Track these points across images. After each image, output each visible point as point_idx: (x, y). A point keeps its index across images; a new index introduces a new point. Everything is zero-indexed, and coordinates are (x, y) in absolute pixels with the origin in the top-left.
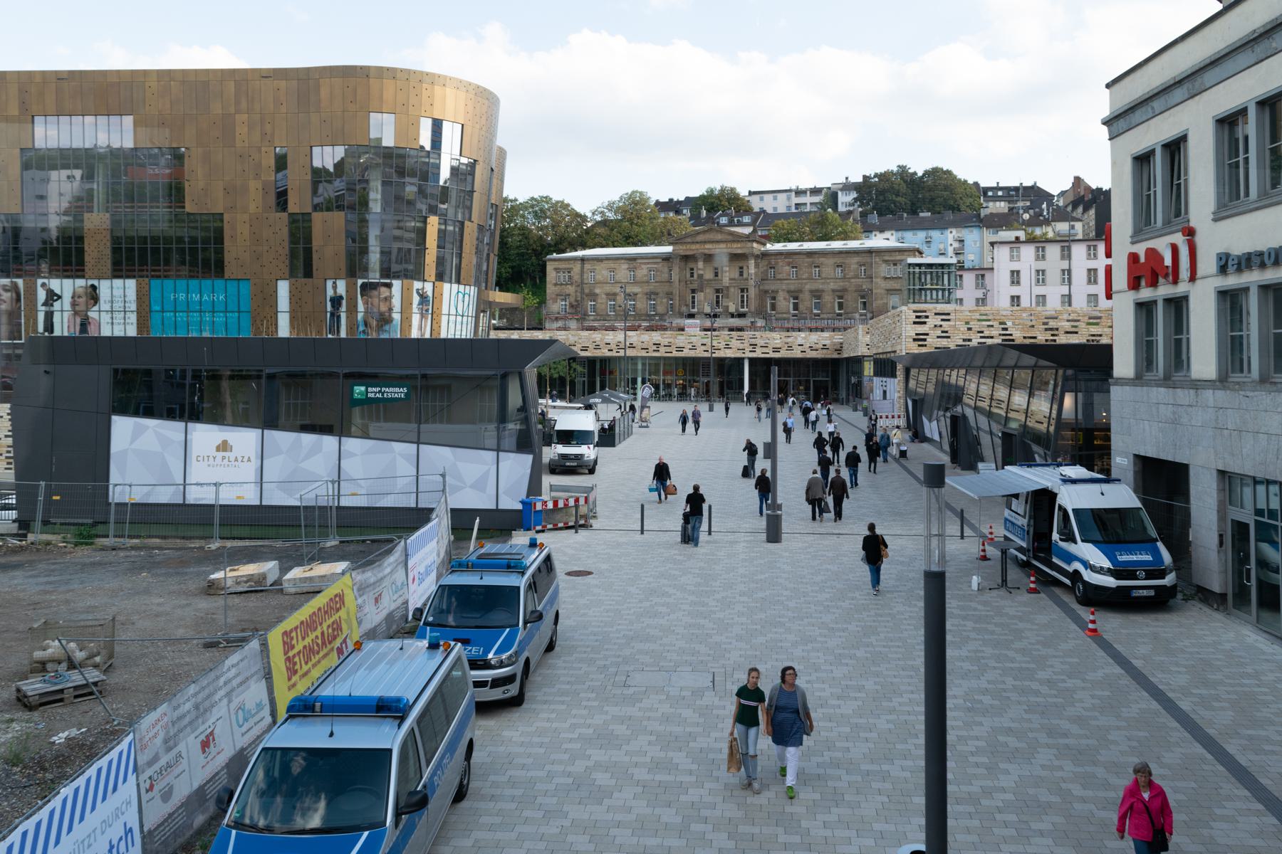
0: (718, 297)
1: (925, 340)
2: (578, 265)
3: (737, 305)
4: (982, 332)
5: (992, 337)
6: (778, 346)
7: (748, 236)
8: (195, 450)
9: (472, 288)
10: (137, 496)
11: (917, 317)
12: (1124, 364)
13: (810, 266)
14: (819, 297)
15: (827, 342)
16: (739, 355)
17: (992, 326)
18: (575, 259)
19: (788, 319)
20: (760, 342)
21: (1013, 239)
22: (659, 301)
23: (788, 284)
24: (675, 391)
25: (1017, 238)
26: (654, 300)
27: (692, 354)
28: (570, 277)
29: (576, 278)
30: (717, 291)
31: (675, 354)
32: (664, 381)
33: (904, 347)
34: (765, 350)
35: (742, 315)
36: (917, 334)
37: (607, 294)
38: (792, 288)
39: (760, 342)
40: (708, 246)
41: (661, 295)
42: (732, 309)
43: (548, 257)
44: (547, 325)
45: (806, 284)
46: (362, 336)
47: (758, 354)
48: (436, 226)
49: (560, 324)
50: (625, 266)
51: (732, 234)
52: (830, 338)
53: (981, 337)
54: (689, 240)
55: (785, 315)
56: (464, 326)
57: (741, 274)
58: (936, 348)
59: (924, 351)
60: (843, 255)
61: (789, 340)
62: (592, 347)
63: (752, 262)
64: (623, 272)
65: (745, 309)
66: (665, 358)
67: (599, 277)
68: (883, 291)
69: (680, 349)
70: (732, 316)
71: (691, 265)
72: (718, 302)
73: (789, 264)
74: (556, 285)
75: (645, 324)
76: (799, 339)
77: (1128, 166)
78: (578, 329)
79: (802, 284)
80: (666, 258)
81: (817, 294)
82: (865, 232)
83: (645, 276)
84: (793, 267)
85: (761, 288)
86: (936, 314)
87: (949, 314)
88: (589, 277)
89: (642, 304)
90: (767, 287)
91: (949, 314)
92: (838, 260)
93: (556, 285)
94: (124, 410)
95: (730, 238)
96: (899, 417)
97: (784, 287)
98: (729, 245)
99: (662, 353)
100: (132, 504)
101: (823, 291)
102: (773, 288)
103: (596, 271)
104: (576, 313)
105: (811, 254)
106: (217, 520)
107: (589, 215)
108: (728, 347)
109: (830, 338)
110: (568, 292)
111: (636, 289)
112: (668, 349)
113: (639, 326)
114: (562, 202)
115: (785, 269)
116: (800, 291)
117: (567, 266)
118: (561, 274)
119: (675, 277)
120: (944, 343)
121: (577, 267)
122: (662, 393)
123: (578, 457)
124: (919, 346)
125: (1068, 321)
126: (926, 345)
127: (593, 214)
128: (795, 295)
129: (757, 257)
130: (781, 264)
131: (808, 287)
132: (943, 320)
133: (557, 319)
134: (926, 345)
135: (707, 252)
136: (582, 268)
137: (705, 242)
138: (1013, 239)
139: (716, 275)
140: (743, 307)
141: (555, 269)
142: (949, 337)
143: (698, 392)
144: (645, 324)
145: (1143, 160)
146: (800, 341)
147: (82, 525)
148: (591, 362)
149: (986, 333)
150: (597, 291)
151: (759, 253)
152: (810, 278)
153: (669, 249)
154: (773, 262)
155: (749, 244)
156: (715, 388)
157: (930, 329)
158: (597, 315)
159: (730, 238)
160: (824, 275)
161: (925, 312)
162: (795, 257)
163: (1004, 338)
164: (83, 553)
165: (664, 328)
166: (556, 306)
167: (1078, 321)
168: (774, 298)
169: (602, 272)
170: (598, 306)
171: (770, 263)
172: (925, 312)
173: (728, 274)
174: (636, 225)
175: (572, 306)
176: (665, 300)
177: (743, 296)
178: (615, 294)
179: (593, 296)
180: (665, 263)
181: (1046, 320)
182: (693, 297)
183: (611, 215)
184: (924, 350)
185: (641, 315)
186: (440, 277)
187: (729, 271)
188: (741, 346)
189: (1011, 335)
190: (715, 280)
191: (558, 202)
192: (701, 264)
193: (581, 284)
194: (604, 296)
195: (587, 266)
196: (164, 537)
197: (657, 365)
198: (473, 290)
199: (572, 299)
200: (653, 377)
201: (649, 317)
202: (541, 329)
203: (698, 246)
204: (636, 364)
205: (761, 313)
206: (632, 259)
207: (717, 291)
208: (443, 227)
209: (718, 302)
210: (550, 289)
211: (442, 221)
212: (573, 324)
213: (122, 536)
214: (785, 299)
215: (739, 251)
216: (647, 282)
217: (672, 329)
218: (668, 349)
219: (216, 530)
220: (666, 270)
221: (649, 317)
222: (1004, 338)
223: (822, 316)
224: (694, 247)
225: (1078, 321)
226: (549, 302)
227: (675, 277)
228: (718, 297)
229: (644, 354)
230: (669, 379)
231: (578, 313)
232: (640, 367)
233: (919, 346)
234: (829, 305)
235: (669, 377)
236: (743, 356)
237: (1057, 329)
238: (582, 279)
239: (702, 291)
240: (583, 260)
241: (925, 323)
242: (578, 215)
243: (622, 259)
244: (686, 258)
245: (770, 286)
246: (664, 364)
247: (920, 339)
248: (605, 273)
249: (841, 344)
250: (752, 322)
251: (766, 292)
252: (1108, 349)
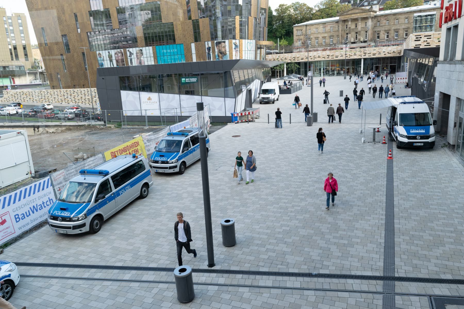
0: (356, 35)
2: (305, 28)
3: (364, 38)
6: (375, 53)
7: (369, 10)
8: (142, 100)
9: (253, 40)
10: (129, 114)
11: (417, 38)
13: (394, 19)
14: (397, 32)
15: (395, 50)
16: (359, 57)
18: (303, 25)
19: (384, 42)
20: (368, 52)
22: (334, 38)
23: (385, 28)
24: (336, 72)
26: (332, 38)
27: (341, 58)
28: (302, 33)
29: (304, 32)
30: (357, 33)
31: (335, 59)
32: (331, 69)
34: (370, 55)
35: (365, 42)
37: (315, 38)
38: (386, 29)
39: (368, 52)
40: (353, 15)
41: (335, 36)
42: (362, 40)
43: (294, 26)
44: (294, 51)
45: (392, 27)
46: (218, 60)
47: (367, 57)
48: (239, 20)
49: (298, 50)
50: (322, 26)
51: (362, 9)
52: (397, 48)
54: (345, 14)
55: (383, 40)
56: (251, 54)
57: (366, 25)
60: (409, 14)
61: (380, 50)
62: (305, 58)
63: (370, 20)
64: (321, 29)
66: (332, 60)
67: (312, 32)
69: (337, 57)
70: (362, 42)
71: (346, 24)
72: (356, 37)
73: (385, 19)
74: (297, 36)
75: (329, 48)
76: (384, 49)
78: (305, 52)
79: (390, 27)
80: (337, 22)
81: (397, 31)
82: (425, 2)
83: (329, 29)
84: (387, 21)
85: (374, 30)
86: (425, 36)
87: (430, 36)
88: (309, 32)
89: (328, 41)
90: (376, 30)
91: (430, 36)
92: (406, 16)
93: (297, 36)
94: (125, 89)
95: (361, 11)
96: (406, 78)
97: (383, 29)
98: (361, 14)
99: (330, 58)
100: (127, 116)
101: (399, 29)
102: (378, 30)
103: (311, 29)
104: (304, 46)
105: (395, 14)
106: (147, 120)
107: (313, 7)
108: (355, 55)
109: (397, 48)
110: (301, 38)
111: (326, 35)
112: (332, 57)
113: (327, 49)
114: (304, 3)
115: (384, 22)
116: (390, 30)
117: (301, 28)
118: (299, 32)
119: (340, 29)
121: (304, 28)
122: (331, 73)
123: (268, 98)
127: (315, 7)
128: (388, 32)
129: (372, 18)
130: (382, 20)
131: (393, 28)
132: (427, 38)
133: (297, 48)
135: (352, 18)
136: (306, 29)
137: (352, 14)
139: (356, 26)
140: (366, 38)
141: (297, 30)
143: (344, 72)
144: (329, 48)
146: (384, 50)
147: (118, 122)
148: (305, 63)
150: (312, 37)
151: (373, 16)
152: (394, 25)
153: (337, 18)
154: (379, 19)
155: (369, 13)
156: (351, 70)
157: (422, 42)
159: (361, 11)
160: (400, 23)
162: (389, 16)
164: (117, 130)
165: (335, 49)
166: (297, 44)
168: (378, 34)
169: (313, 29)
170: (312, 42)
171: (378, 20)
172: (420, 35)
173: (360, 26)
174: (331, 9)
175: (302, 43)
176: (336, 38)
177: (366, 34)
178: (318, 38)
179: (310, 39)
180: (337, 24)
182: (347, 36)
183: (322, 7)
185: (328, 44)
186: (241, 38)
187: (361, 25)
188: (360, 54)
190: (355, 29)
191: (302, 4)
192: (350, 23)
193: (306, 35)
194: (314, 39)
195: (308, 28)
196: (138, 125)
197: (329, 63)
198: (254, 42)
199: (303, 41)
200: (328, 68)
201: (330, 45)
202: (292, 52)
203: (349, 16)
204: (321, 63)
205: (373, 40)
206: (324, 23)
207: (357, 33)
208: (241, 19)
209: (356, 37)
210: (295, 38)
211: (241, 17)
212: (303, 50)
213: (125, 125)
214: (383, 34)
215: (365, 16)
216: (330, 32)
217: (338, 49)
218: (332, 57)
219: (147, 123)
220: (337, 26)
221: (330, 45)
223: (398, 39)
224: (347, 16)
226: (295, 42)
227: (340, 29)
228: (356, 35)
229: (323, 59)
230: (333, 68)
231: (305, 46)
232: (322, 64)
234: (401, 35)
235: (333, 67)
236: (361, 58)
238: (306, 33)
239: (350, 33)
240: (306, 25)
242: (309, 8)
243: (320, 24)
244: (345, 21)
245: (377, 29)
246: (332, 63)
248: (314, 30)
249: (401, 50)
250: (369, 44)
251: (375, 32)
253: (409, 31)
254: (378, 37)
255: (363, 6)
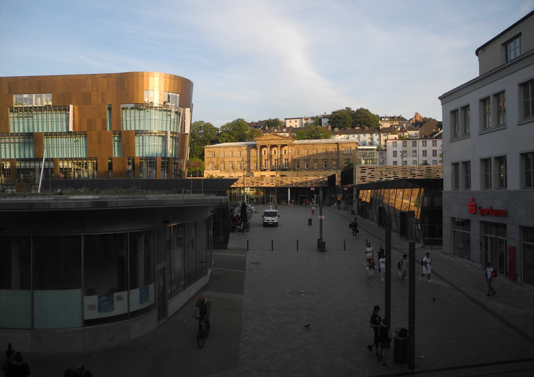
1: (365, 179)
4: (387, 176)
5: (390, 178)
12: (447, 186)
17: (390, 173)
18: (217, 147)
21: (394, 139)
25: (395, 138)
27: (267, 186)
33: (357, 182)
36: (362, 177)
53: (386, 178)
58: (369, 182)
59: (364, 183)
65: (287, 167)
68: (343, 160)
77: (449, 114)
86: (369, 169)
87: (374, 169)
91: (374, 169)
101: (318, 160)
105: (313, 144)
110: (214, 161)
120: (372, 180)
124: (363, 181)
125: (419, 171)
126: (365, 181)
130: (301, 149)
132: (371, 171)
134: (365, 181)
138: (394, 139)
142: (374, 178)
145: (454, 112)
149: (389, 176)
150: (226, 160)
158: (226, 170)
161: (365, 168)
163: (395, 178)
167: (423, 171)
168: (298, 163)
170: (226, 167)
172: (365, 168)
181: (411, 171)
184: (364, 183)
189: (398, 176)
214: (303, 163)
222: (395, 178)
225: (423, 171)
233: (363, 181)
236: (288, 186)
237: (415, 174)
241: (365, 172)
247: (363, 178)
252: (441, 181)
253: (328, 162)
254: (298, 166)
255: (282, 132)
